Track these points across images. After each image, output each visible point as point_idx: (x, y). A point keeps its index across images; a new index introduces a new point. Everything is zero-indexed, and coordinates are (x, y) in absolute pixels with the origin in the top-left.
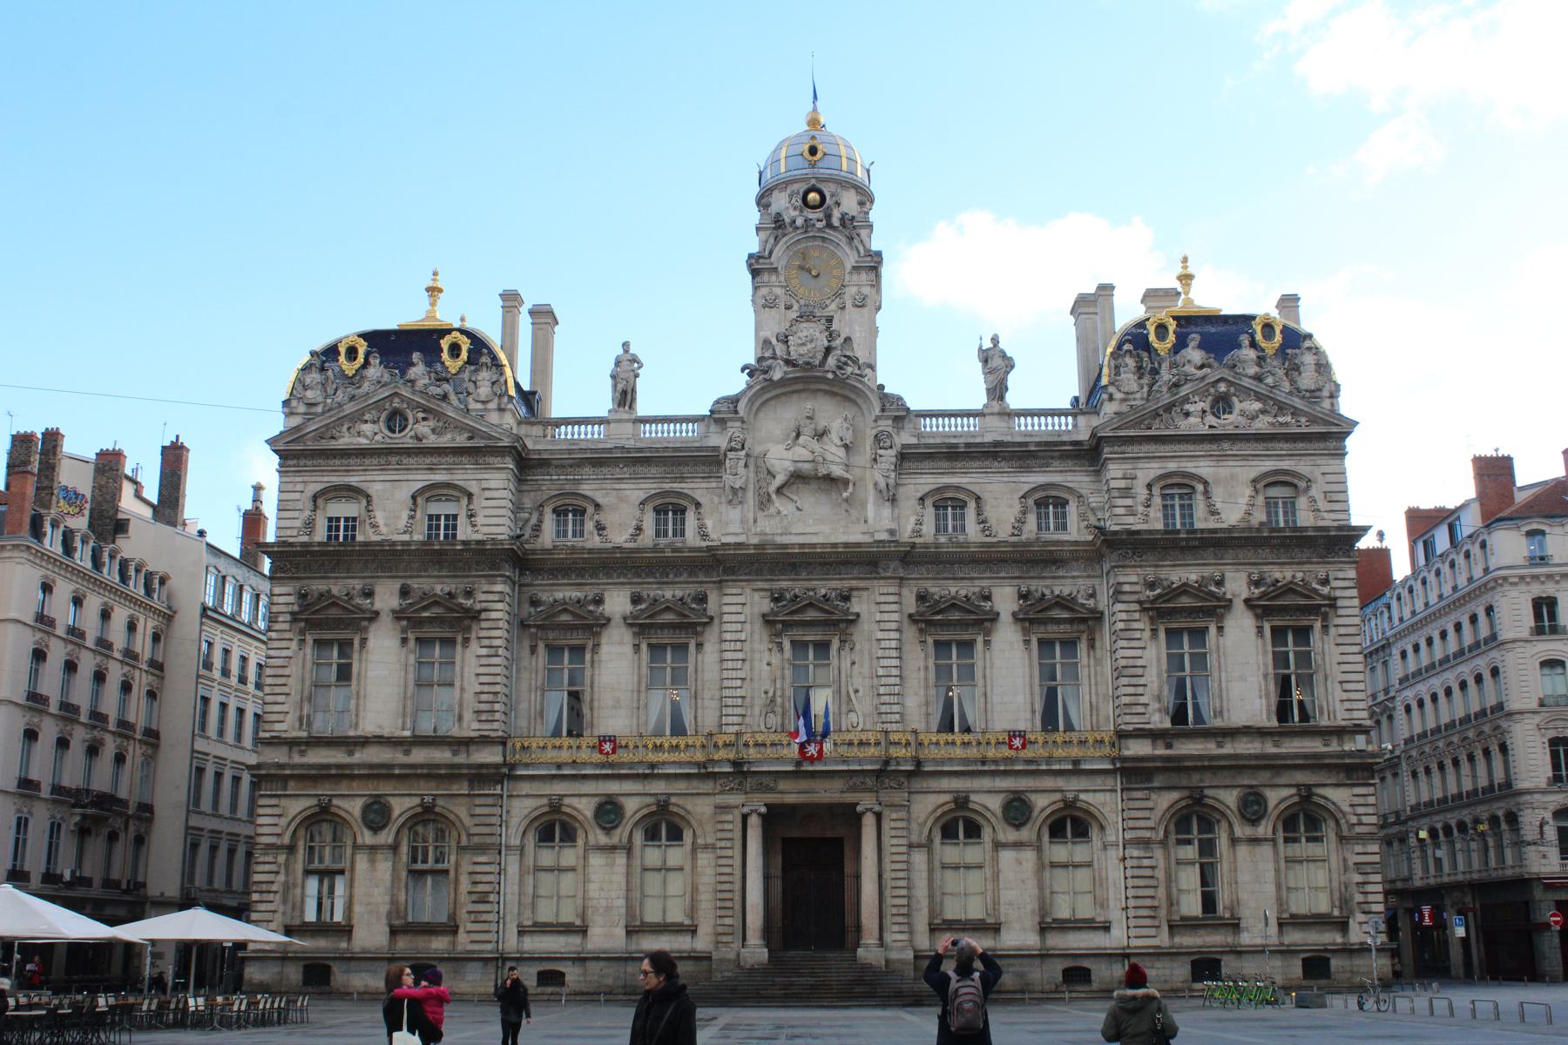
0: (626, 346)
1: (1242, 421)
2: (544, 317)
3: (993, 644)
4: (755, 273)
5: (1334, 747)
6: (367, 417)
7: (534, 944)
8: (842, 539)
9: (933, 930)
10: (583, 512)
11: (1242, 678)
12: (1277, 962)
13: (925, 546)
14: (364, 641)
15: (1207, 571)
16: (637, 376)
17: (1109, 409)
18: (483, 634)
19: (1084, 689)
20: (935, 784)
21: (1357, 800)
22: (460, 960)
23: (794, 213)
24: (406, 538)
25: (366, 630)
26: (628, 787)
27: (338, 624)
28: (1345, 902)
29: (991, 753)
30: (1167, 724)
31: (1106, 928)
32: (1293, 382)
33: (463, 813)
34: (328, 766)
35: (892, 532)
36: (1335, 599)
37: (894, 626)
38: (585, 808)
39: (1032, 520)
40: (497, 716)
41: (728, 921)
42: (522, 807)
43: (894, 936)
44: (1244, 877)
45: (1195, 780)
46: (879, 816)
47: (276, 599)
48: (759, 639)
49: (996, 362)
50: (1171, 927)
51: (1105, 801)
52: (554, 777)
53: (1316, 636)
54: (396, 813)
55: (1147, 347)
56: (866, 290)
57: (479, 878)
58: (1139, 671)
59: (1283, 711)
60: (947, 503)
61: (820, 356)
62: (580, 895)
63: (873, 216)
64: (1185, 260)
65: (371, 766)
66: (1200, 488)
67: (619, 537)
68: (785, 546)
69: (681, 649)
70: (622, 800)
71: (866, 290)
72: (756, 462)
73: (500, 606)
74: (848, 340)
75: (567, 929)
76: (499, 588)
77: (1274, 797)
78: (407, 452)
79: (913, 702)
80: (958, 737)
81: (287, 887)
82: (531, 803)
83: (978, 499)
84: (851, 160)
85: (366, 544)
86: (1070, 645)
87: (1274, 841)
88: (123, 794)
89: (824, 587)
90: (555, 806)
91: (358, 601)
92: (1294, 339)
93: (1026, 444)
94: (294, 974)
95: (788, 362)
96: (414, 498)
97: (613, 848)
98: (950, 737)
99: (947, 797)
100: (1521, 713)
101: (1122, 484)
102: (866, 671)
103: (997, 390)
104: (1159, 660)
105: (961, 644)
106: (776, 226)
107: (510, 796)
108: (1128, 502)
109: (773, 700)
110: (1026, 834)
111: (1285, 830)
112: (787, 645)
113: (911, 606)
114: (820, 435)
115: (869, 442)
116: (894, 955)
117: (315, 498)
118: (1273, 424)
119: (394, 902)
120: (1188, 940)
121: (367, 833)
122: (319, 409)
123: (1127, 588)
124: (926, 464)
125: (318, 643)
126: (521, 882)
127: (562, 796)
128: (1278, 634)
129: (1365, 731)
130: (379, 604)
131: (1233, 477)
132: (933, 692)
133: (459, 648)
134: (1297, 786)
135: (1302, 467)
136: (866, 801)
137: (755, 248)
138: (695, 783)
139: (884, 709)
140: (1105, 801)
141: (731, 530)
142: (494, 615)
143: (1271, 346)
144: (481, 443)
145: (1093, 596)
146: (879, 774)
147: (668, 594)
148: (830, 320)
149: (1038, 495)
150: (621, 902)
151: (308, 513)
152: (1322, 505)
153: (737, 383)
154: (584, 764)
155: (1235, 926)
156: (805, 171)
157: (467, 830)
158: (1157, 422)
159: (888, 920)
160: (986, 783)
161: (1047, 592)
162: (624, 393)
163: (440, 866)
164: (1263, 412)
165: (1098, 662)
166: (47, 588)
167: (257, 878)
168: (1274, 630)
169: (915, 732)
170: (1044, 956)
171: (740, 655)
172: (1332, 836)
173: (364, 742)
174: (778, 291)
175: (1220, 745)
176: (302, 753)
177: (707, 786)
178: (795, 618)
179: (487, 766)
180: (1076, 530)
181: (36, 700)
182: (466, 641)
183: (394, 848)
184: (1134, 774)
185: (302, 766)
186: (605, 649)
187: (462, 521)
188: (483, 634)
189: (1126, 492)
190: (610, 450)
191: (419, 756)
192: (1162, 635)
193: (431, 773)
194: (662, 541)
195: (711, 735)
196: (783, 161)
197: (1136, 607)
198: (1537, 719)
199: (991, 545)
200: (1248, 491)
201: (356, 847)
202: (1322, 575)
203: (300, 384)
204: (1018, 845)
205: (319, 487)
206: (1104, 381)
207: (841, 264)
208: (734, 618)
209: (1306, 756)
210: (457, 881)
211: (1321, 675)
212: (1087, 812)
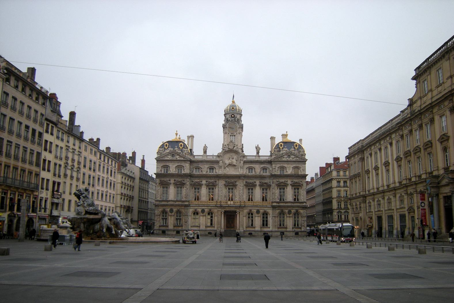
0: (205, 145)
1: (292, 159)
2: (192, 137)
3: (256, 189)
4: (224, 128)
5: (301, 205)
6: (169, 155)
7: (192, 228)
8: (235, 174)
9: (246, 227)
10: (199, 169)
11: (289, 195)
12: (292, 233)
13: (247, 175)
14: (169, 187)
15: (285, 180)
16: (207, 149)
17: (273, 157)
18: (186, 186)
19: (268, 196)
20: (247, 208)
21: (304, 212)
22: (183, 231)
23: (230, 119)
24: (175, 173)
25: (169, 185)
26: (206, 207)
27: (165, 184)
28: (301, 225)
29: (255, 204)
30: (279, 201)
31: (269, 228)
32: (299, 153)
33: (183, 211)
34: (165, 204)
35: (242, 173)
36: (303, 184)
37: (242, 186)
38: (200, 210)
39: (262, 171)
40: (188, 198)
41: (219, 226)
42: (191, 210)
43: (241, 228)
44: (288, 221)
45: (282, 208)
46: (239, 212)
47: (157, 181)
48: (224, 187)
49: (258, 149)
50: (278, 228)
51: (270, 211)
52: (195, 206)
53: (300, 189)
54: (174, 211)
55: (279, 148)
56: (241, 131)
57: (185, 220)
58: (275, 194)
59: (295, 199)
60: (250, 169)
61: (233, 148)
62: (199, 222)
63: (242, 119)
64: (287, 132)
65: (170, 204)
66: (285, 168)
67: (204, 173)
68: (227, 175)
69: (213, 189)
70: (205, 209)
71: (241, 131)
72: (223, 162)
73: (188, 182)
74: (237, 145)
75: (197, 226)
76: (188, 180)
77: (292, 211)
78: (175, 160)
79: (244, 197)
80: (250, 201)
81: (159, 221)
82: (192, 210)
83: (254, 168)
84: (239, 109)
85: (169, 174)
86: (266, 189)
87: (292, 217)
88: (130, 206)
89: (233, 180)
90: (196, 210)
91: (168, 181)
92: (300, 147)
93: (261, 161)
94: (161, 232)
95: (228, 148)
96: (176, 167)
97: (204, 216)
98: (249, 202)
99: (249, 210)
100: (334, 198)
101: (274, 167)
102: (238, 192)
103: (258, 153)
104: (278, 192)
105: (251, 189)
106: (227, 120)
107: (190, 209)
108: (275, 170)
109: (225, 196)
110: (259, 215)
111: (294, 215)
112: (227, 188)
113: (245, 183)
114: (233, 158)
115: (240, 160)
116: (241, 231)
117: (162, 167)
118: (296, 160)
119: (174, 223)
120: (280, 230)
121: (170, 213)
122: (162, 154)
123: (274, 182)
124: (248, 163)
125: (163, 187)
126: (191, 220)
127: (196, 209)
128: (295, 189)
129: (306, 202)
130: (171, 182)
131: (290, 167)
132: (247, 195)
133: (182, 188)
134: (296, 210)
135: (300, 166)
136: (238, 210)
137: (224, 123)
138: (215, 207)
139: (240, 197)
140: (270, 211)
141: (220, 172)
142: (187, 184)
143: (296, 148)
144: (185, 159)
145: (270, 182)
146: (239, 207)
147: (211, 181)
148: (235, 136)
149: (263, 168)
150: (205, 223)
151: (161, 169)
152: (302, 171)
153: (220, 150)
154: (199, 205)
155: (286, 228)
156: (232, 112)
157: (184, 213)
158: (280, 159)
159: (240, 226)
160: (254, 208)
161: (264, 182)
162: (205, 152)
163: (180, 218)
164: (295, 158)
165: (270, 192)
166: (122, 178)
167: (155, 219)
168: (294, 188)
169: (244, 201)
170: (261, 231)
171: (221, 190)
172: (300, 216)
173: (170, 201)
174: (227, 131)
175: (286, 204)
176: (161, 202)
177: (217, 208)
178: (229, 185)
179: (187, 205)
180: (268, 174)
181: (122, 193)
182: (183, 187)
183: (174, 215)
184: (274, 207)
185: (160, 204)
186: (202, 188)
187: (183, 170)
188: (186, 186)
189: (275, 169)
190: (203, 160)
191: (177, 203)
192: (279, 189)
193: (179, 205)
194: (210, 174)
195: (217, 201)
196: (228, 110)
197: (275, 185)
198: (336, 199)
199: (257, 175)
200: (292, 169)
201: (169, 215)
202: (301, 181)
203: (159, 150)
204: (258, 216)
205: (162, 165)
206: (273, 153)
207: (237, 127)
208: (220, 184)
209: (297, 206)
210: (182, 220)
211: (300, 195)
212: (267, 212)
